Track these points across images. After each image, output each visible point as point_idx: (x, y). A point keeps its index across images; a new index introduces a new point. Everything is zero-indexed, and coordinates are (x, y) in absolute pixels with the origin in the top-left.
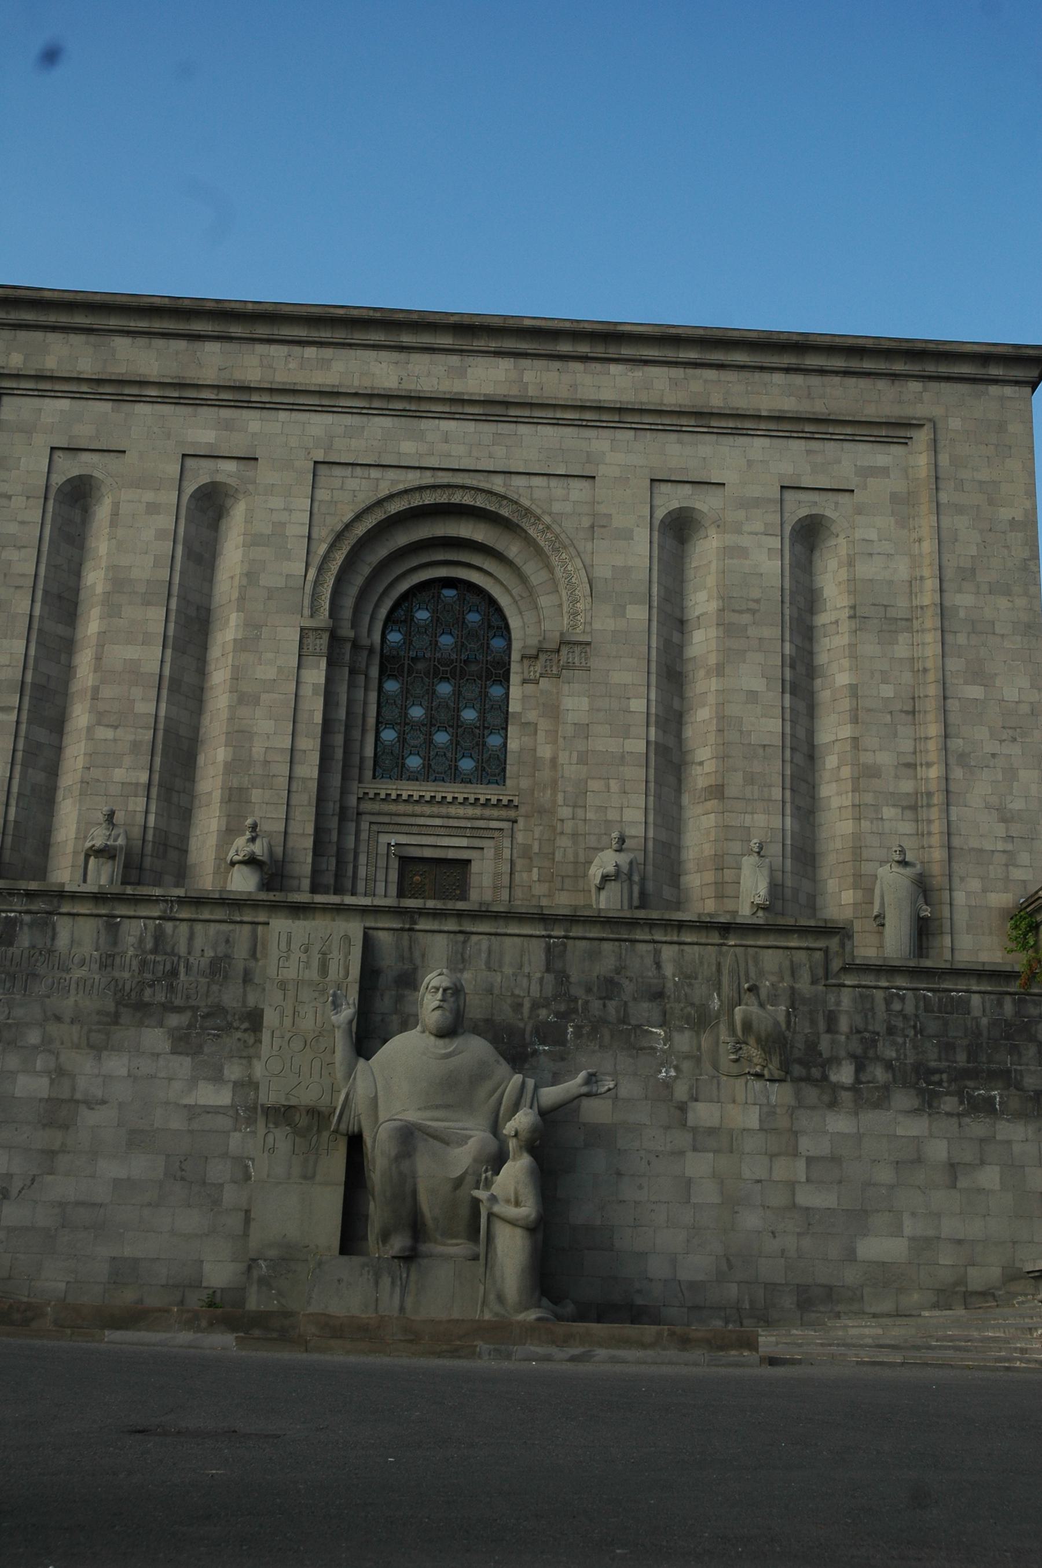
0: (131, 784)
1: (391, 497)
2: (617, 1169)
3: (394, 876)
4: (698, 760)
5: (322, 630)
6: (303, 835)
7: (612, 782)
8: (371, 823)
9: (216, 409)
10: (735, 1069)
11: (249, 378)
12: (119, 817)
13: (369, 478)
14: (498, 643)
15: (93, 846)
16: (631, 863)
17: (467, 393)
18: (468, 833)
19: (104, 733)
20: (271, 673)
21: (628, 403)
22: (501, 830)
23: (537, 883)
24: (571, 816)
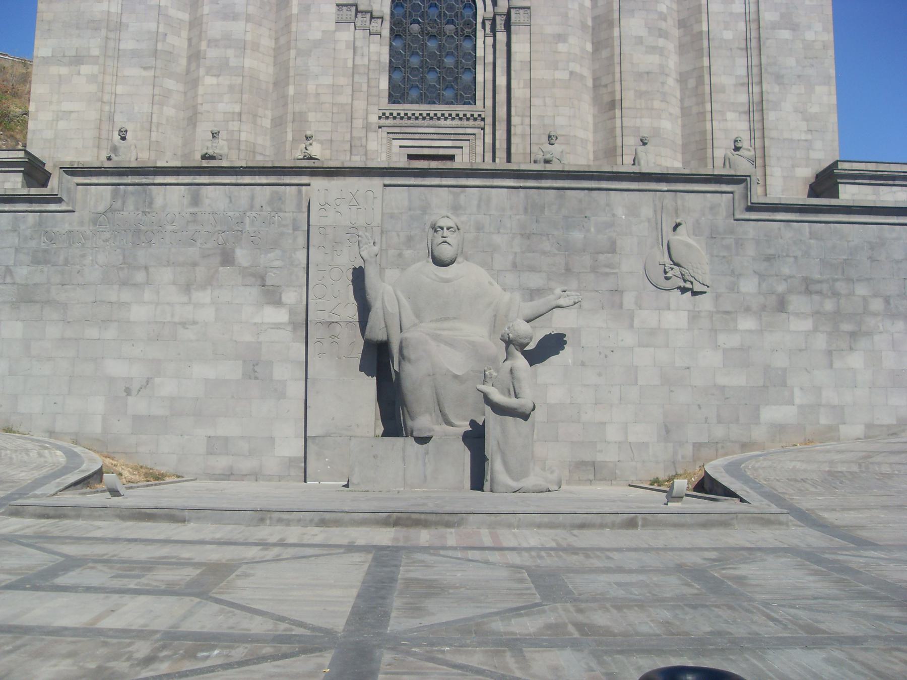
0: (229, 113)
2: (582, 362)
4: (603, 83)
8: (388, 133)
10: (668, 284)
12: (223, 135)
14: (468, 13)
15: (207, 154)
16: (562, 152)
18: (452, 137)
19: (209, 80)
20: (318, 35)
22: (474, 134)
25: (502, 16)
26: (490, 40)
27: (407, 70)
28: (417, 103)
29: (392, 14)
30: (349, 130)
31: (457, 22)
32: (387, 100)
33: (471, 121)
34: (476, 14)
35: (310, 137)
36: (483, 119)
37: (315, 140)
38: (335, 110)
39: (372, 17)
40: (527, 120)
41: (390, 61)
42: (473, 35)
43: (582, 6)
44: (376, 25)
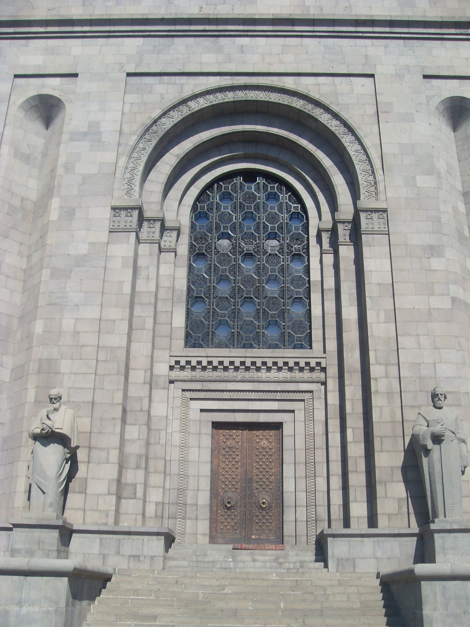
1: (194, 97)
3: (207, 441)
5: (133, 208)
6: (112, 404)
7: (422, 338)
9: (45, 40)
11: (72, 13)
13: (175, 84)
16: (456, 419)
17: (258, 14)
18: (278, 396)
20: (83, 249)
21: (396, 16)
22: (311, 392)
23: (353, 443)
24: (384, 375)
25: (347, 224)
26: (329, 259)
27: (212, 300)
28: (227, 347)
29: (193, 227)
30: (122, 387)
31: (281, 236)
32: (182, 342)
33: (305, 372)
34: (308, 226)
35: (55, 399)
36: (324, 370)
37: (69, 401)
38: (102, 356)
39: (163, 229)
40: (394, 370)
41: (189, 289)
42: (304, 253)
43: (455, 209)
44: (170, 239)
